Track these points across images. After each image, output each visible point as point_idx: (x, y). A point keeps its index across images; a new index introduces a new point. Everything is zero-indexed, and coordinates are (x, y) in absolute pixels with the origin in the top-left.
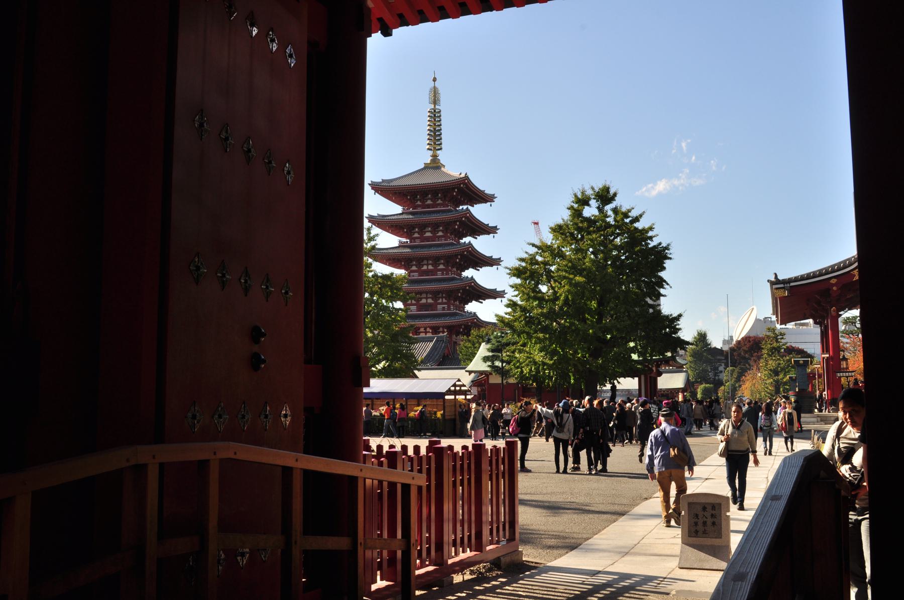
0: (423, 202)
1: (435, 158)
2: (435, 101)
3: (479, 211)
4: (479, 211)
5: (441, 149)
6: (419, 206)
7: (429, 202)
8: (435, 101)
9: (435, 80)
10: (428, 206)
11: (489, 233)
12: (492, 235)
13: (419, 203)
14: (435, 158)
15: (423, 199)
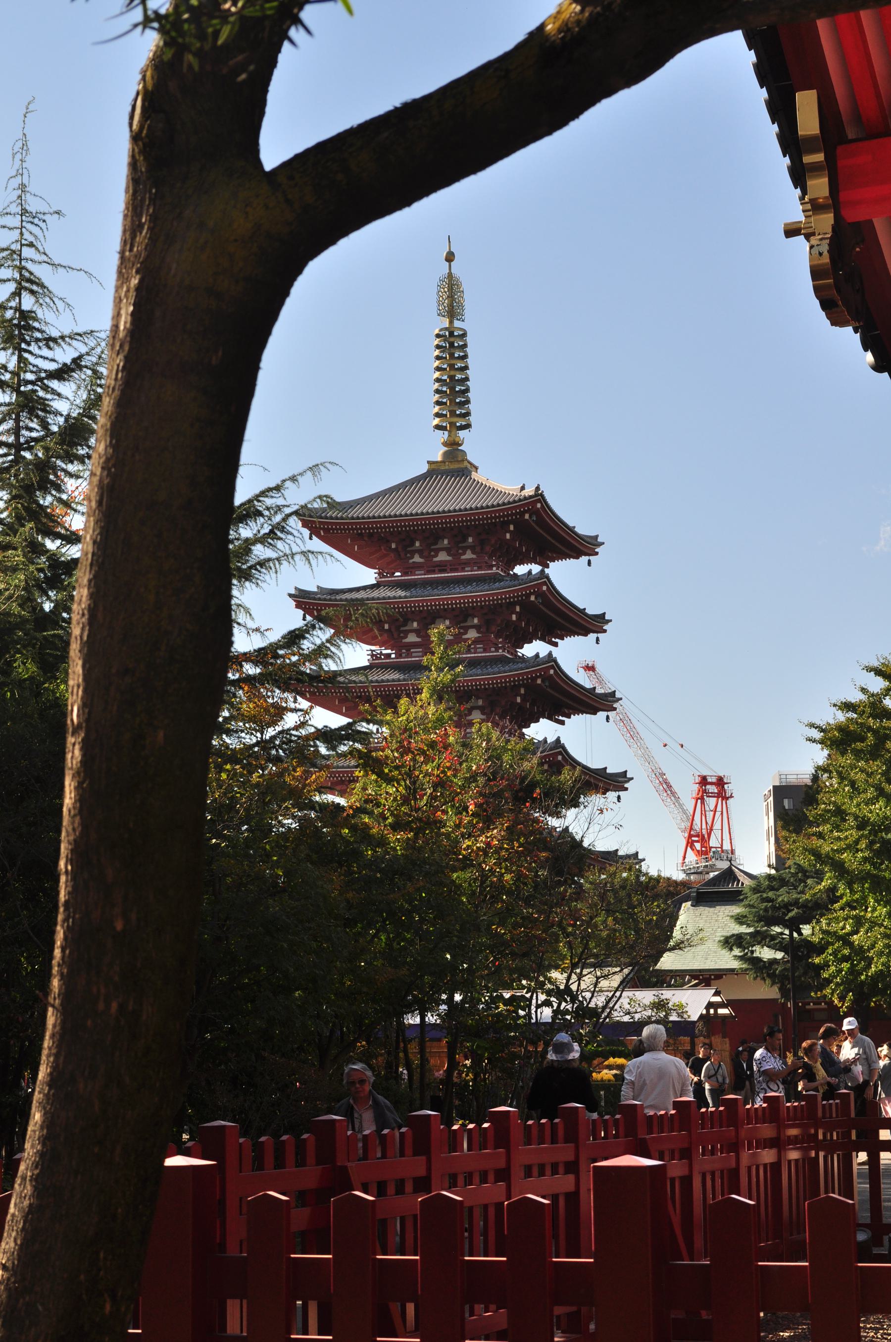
0: (428, 558)
1: (454, 448)
2: (452, 308)
3: (567, 577)
4: (567, 577)
5: (468, 426)
6: (418, 566)
7: (443, 557)
8: (452, 308)
9: (450, 257)
10: (442, 567)
11: (585, 632)
12: (592, 636)
13: (417, 559)
14: (454, 448)
15: (429, 551)
